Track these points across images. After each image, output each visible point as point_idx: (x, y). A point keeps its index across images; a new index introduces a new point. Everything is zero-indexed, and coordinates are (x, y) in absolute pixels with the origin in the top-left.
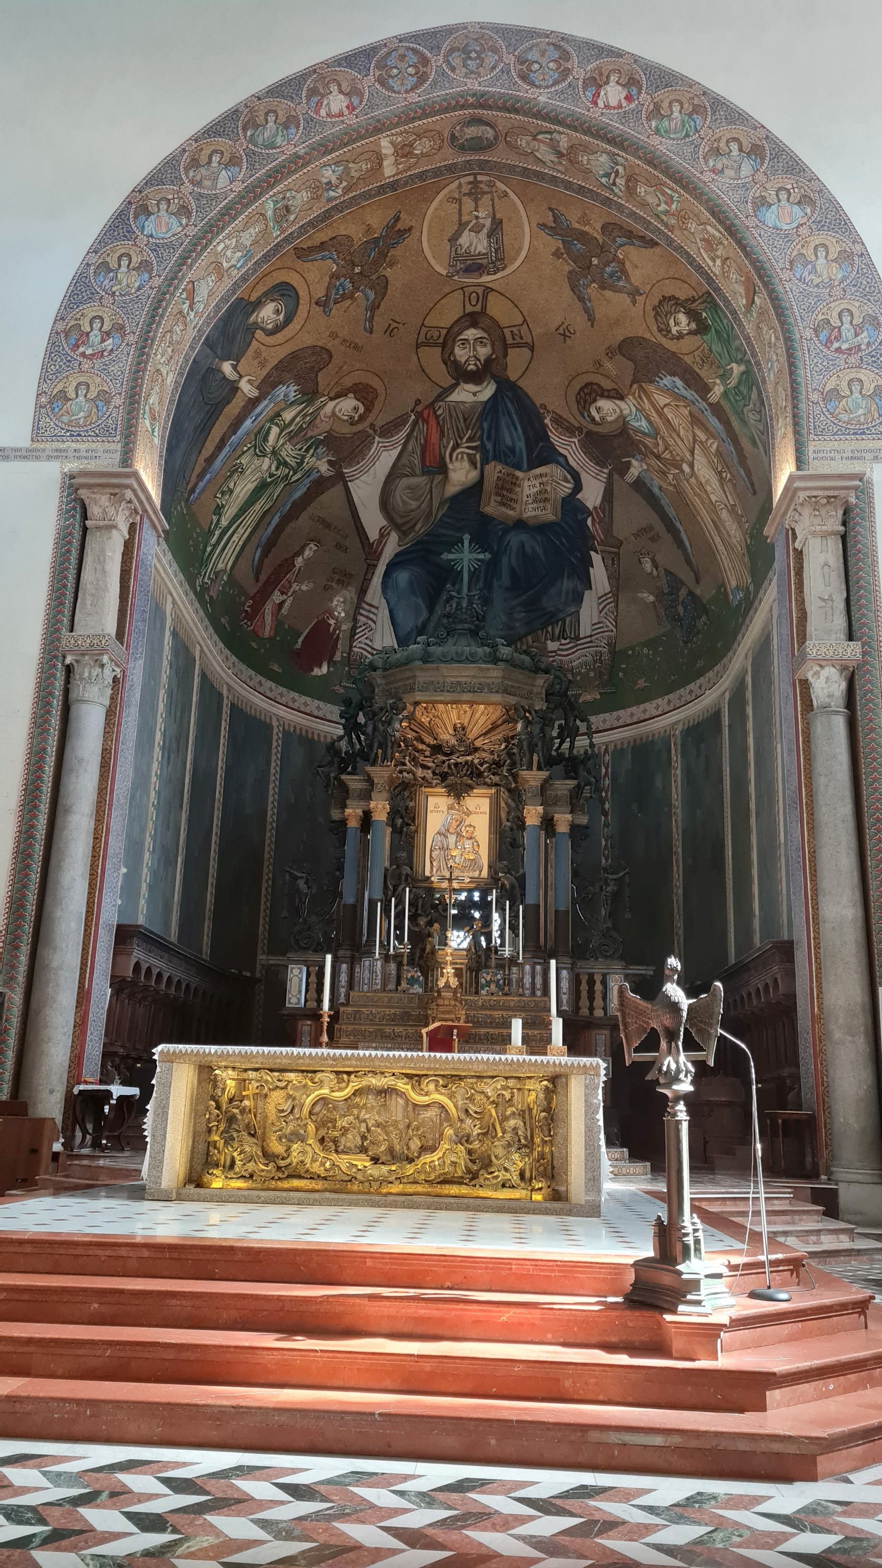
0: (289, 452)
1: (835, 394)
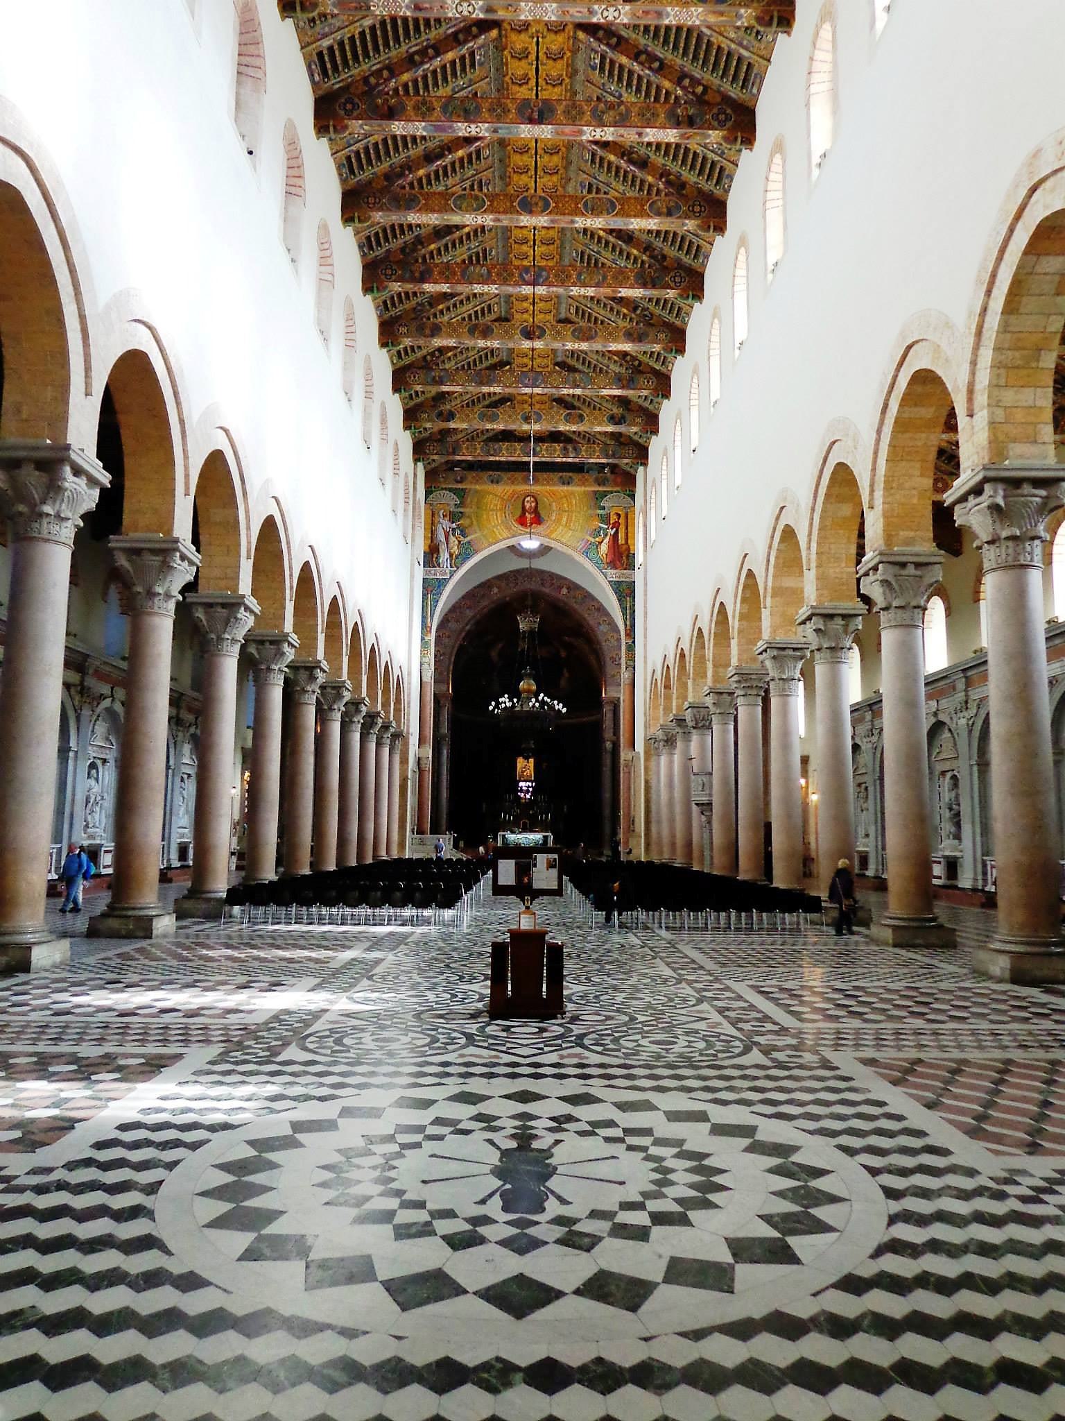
1: (614, 676)
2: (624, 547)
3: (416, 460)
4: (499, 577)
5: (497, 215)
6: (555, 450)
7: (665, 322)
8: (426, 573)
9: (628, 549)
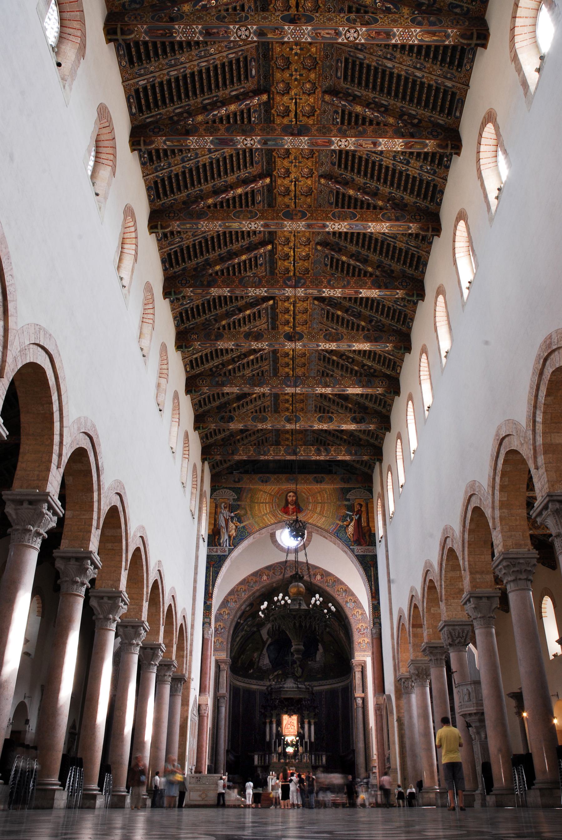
0: (248, 629)
2: (367, 528)
3: (203, 460)
4: (268, 568)
5: (266, 221)
6: (311, 451)
7: (393, 329)
8: (209, 550)
9: (370, 530)
